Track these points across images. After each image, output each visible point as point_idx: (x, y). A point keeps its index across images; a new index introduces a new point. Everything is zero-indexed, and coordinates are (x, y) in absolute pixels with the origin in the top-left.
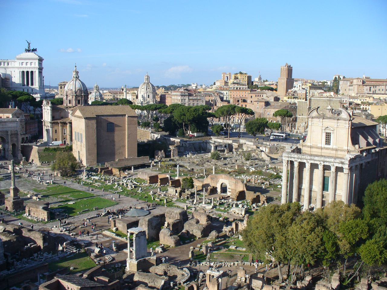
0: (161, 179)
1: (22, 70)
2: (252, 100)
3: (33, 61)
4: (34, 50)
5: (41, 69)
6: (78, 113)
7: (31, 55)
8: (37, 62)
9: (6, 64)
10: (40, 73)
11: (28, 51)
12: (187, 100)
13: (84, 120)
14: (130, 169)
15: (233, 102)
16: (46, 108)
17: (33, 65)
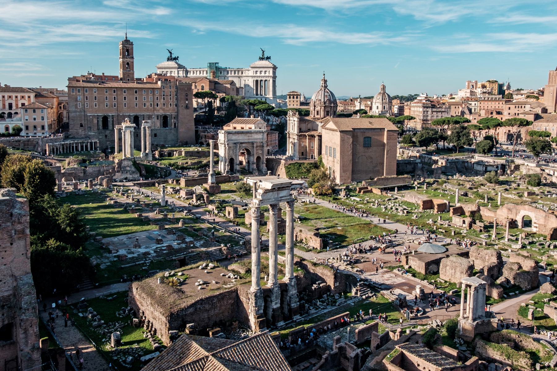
0: (438, 205)
1: (255, 79)
2: (509, 111)
3: (267, 70)
4: (268, 58)
5: (274, 77)
6: (331, 125)
7: (265, 63)
8: (271, 70)
9: (240, 73)
10: (274, 82)
11: (262, 59)
12: (430, 113)
13: (339, 133)
14: (392, 189)
15: (486, 114)
16: (291, 119)
17: (267, 74)
